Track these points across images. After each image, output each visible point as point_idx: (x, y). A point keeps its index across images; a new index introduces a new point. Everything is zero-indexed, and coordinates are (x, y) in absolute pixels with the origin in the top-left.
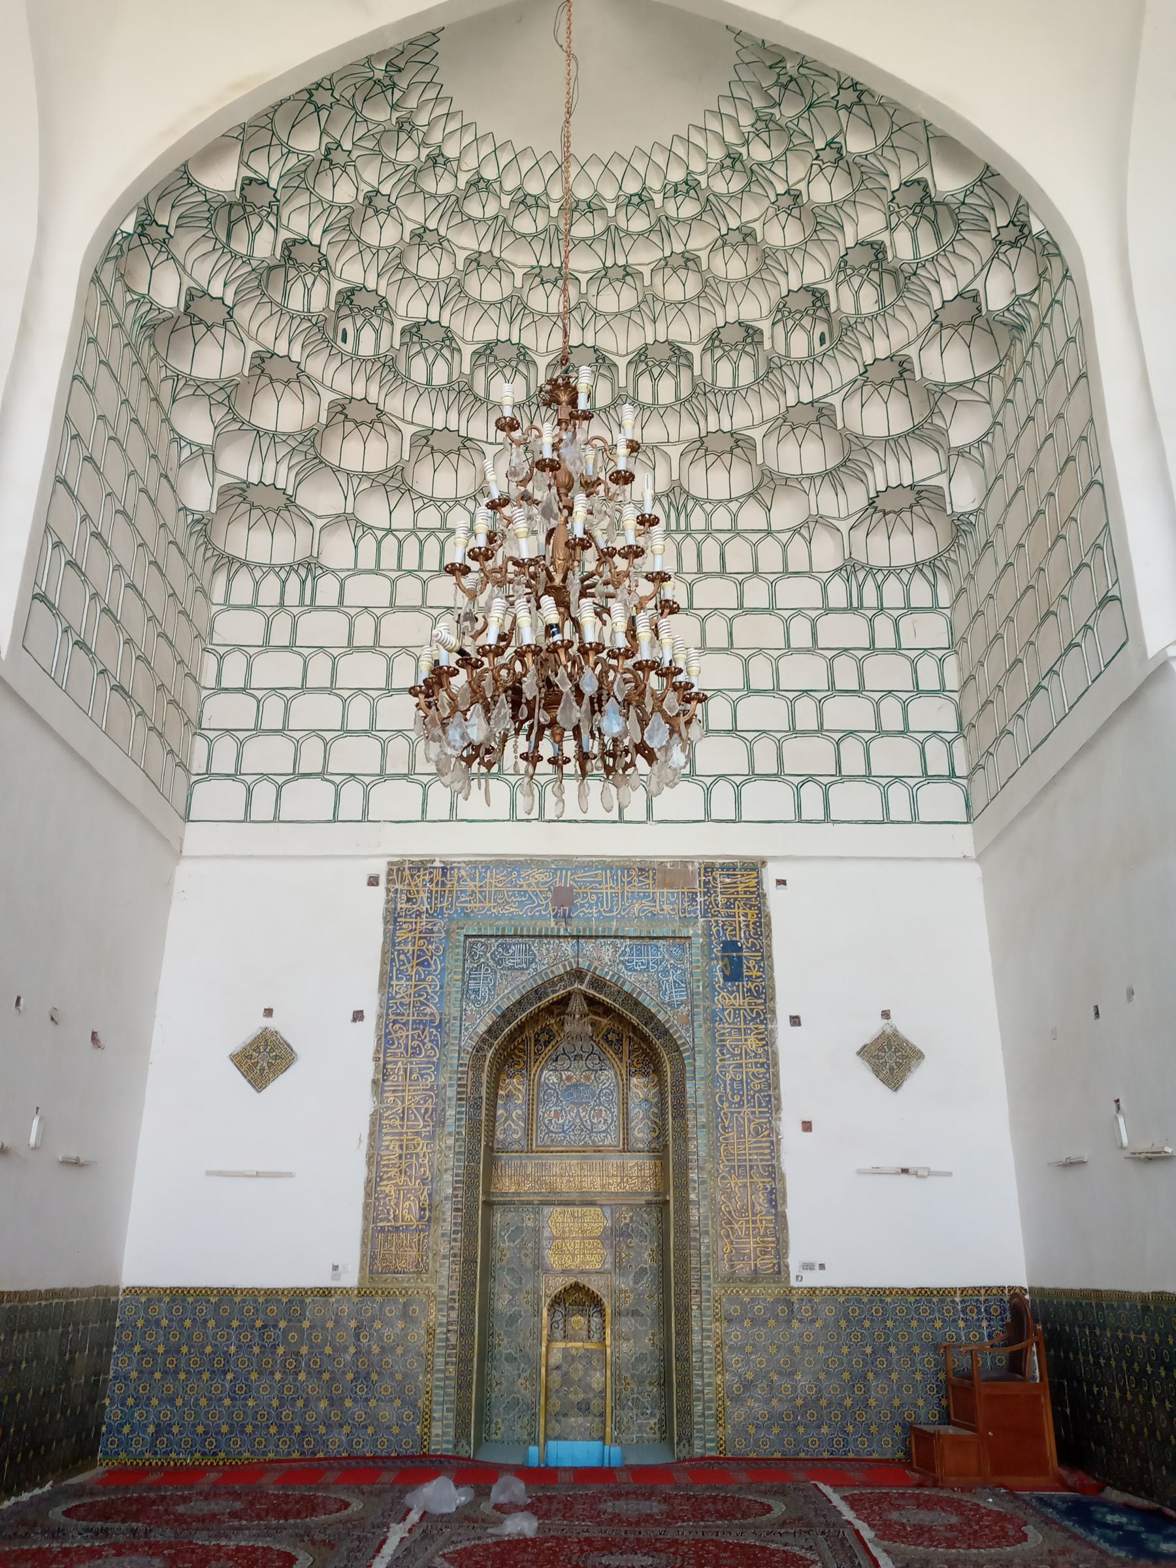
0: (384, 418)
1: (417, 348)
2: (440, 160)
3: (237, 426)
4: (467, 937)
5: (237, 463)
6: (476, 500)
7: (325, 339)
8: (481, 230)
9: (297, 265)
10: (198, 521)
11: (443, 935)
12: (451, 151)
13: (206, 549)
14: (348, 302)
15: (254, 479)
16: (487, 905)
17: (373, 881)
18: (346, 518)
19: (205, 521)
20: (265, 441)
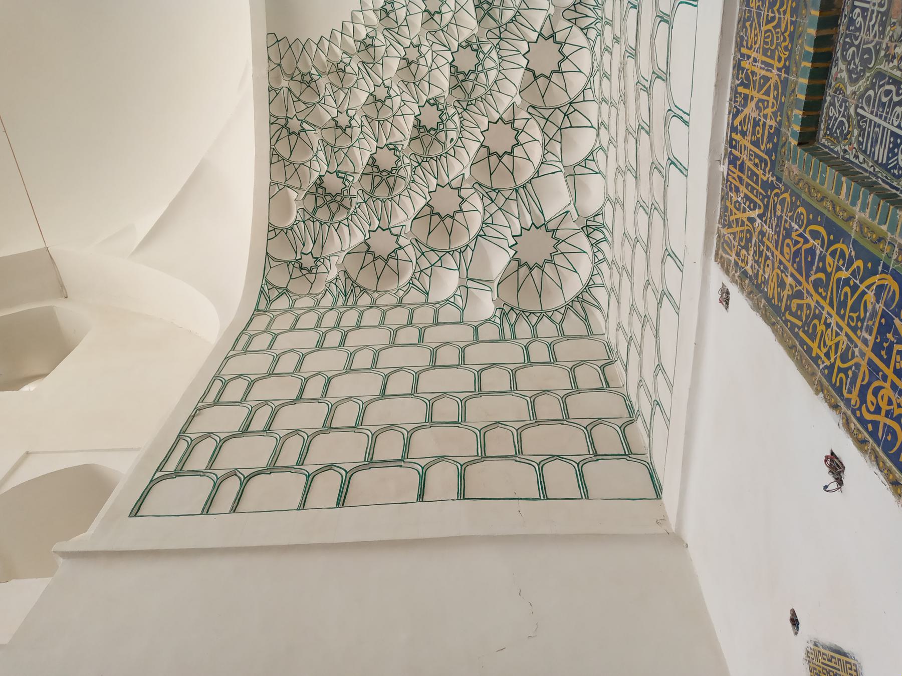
0: (506, 117)
1: (482, 75)
2: (369, 41)
3: (469, 251)
4: (807, 139)
5: (499, 261)
6: (587, 28)
7: (438, 158)
8: (414, 9)
9: (397, 168)
10: (504, 315)
11: (786, 195)
12: (363, 32)
13: (550, 318)
14: (432, 132)
15: (512, 252)
16: (774, 75)
17: (725, 299)
18: (572, 175)
19: (507, 309)
20: (489, 231)
